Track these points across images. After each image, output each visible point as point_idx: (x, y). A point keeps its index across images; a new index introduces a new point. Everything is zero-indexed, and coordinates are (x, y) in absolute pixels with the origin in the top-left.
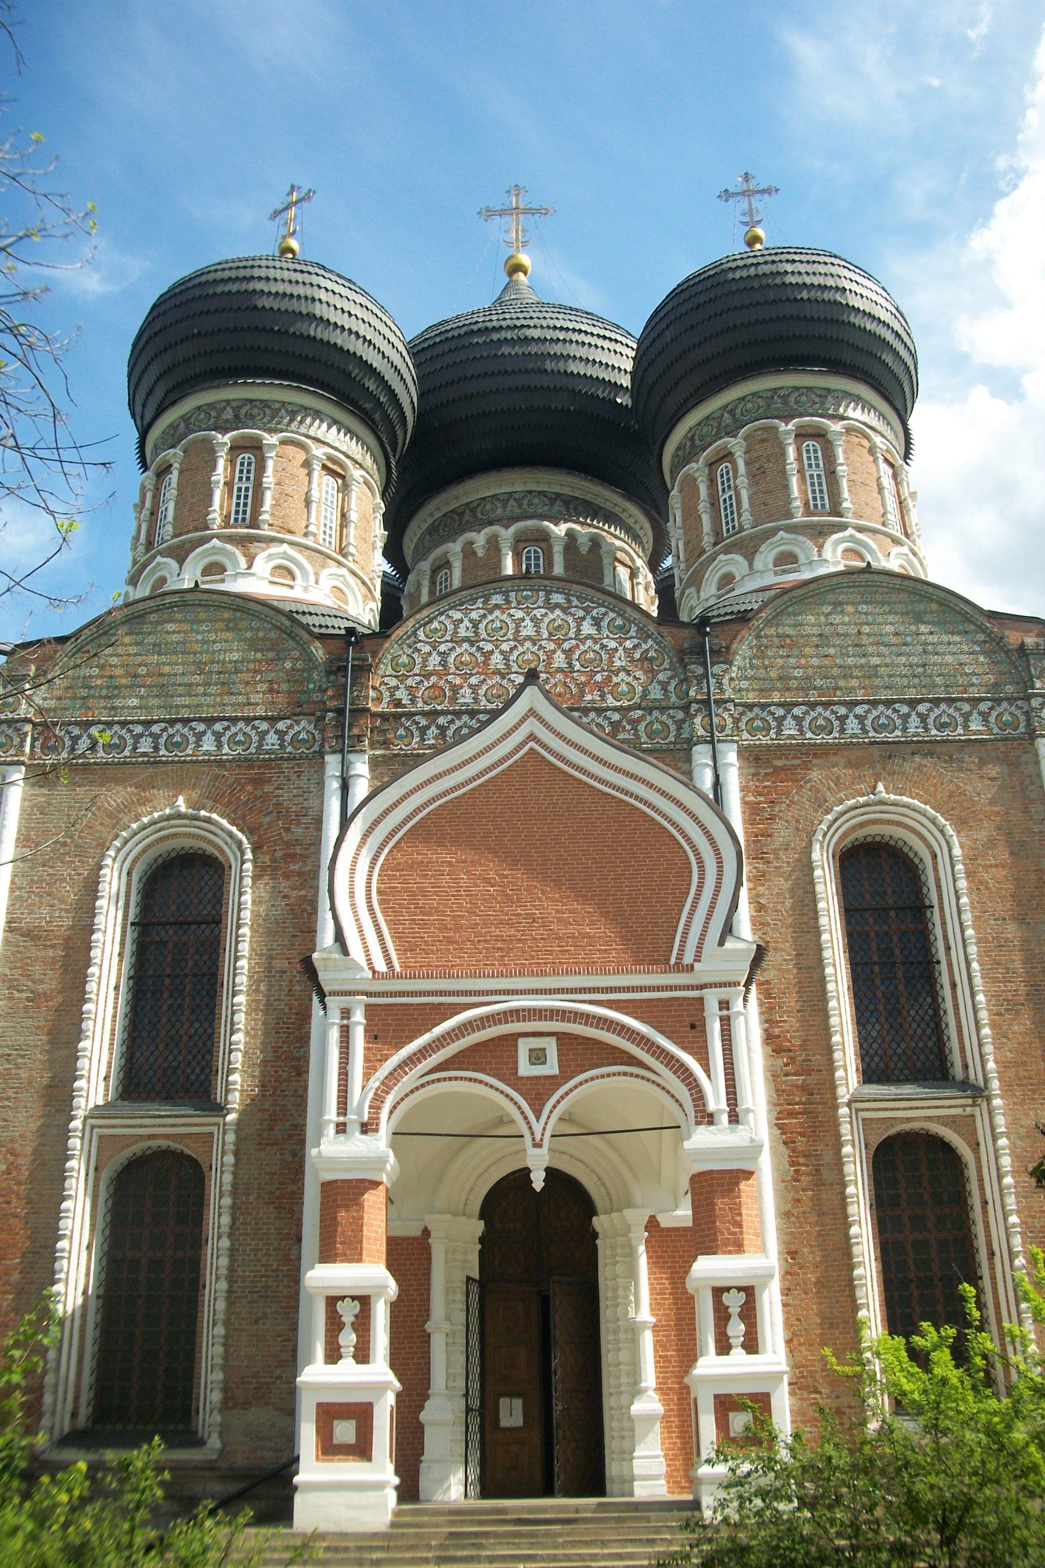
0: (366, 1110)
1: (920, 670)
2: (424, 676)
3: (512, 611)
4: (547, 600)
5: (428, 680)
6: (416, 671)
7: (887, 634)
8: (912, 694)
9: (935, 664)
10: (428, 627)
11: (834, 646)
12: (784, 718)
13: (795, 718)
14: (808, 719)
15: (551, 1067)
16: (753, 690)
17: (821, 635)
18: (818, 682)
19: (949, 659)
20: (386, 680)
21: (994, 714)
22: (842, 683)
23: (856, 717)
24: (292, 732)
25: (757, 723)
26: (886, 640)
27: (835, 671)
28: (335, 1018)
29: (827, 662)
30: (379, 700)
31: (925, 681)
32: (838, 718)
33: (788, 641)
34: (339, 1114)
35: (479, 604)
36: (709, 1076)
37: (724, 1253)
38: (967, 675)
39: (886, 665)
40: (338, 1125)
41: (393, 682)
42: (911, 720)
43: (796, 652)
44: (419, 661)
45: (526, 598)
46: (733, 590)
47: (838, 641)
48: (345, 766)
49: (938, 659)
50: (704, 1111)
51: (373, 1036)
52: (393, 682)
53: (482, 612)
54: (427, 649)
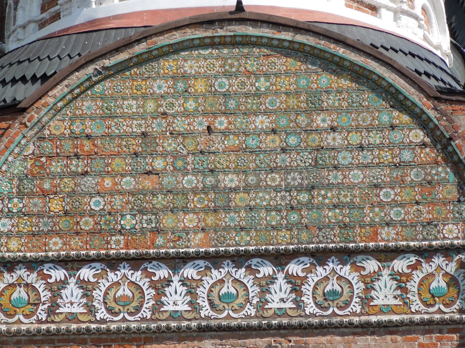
1: (304, 197)
7: (258, 133)
8: (283, 241)
9: (329, 186)
11: (164, 155)
12: (63, 283)
13: (83, 284)
14: (104, 284)
16: (19, 235)
17: (144, 134)
18: (128, 222)
19: (356, 176)
21: (418, 276)
22: (168, 221)
23: (183, 282)
25: (20, 293)
26: (252, 142)
27: (160, 201)
29: (148, 183)
31: (309, 216)
32: (153, 285)
33: (87, 146)
38: (381, 205)
42: (274, 287)
43: (98, 165)
46: (56, 17)
47: (170, 145)
49: (334, 177)
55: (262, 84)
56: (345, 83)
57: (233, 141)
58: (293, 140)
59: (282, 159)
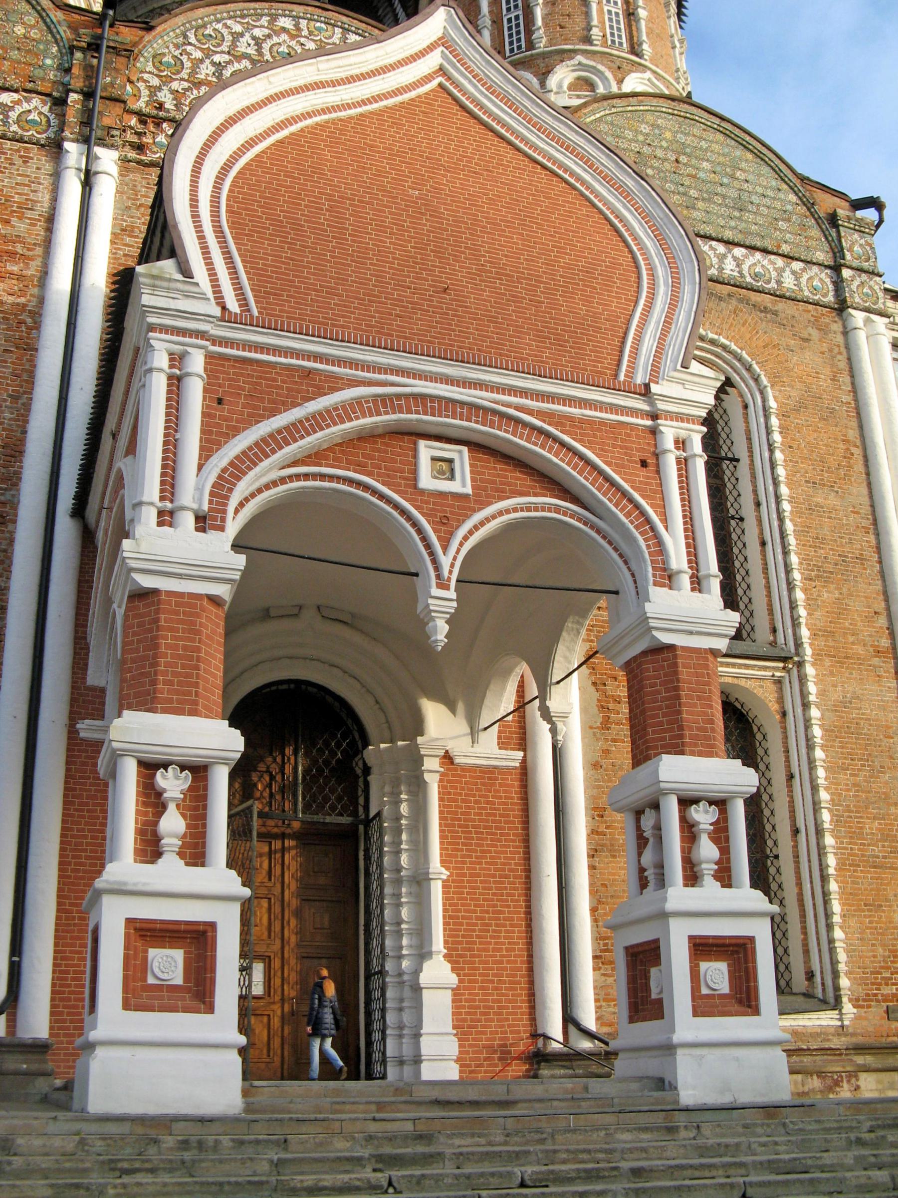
0: (206, 497)
2: (194, 84)
3: (302, 40)
4: (344, 39)
5: (198, 89)
6: (184, 74)
8: (728, 234)
10: (200, 31)
15: (463, 484)
20: (146, 76)
24: (19, 109)
28: (160, 360)
30: (137, 96)
34: (162, 499)
35: (264, 21)
36: (666, 528)
37: (692, 754)
39: (703, 199)
40: (161, 513)
41: (155, 82)
44: (187, 64)
45: (319, 30)
48: (90, 157)
50: (665, 570)
51: (215, 399)
52: (155, 82)
53: (267, 31)
54: (198, 54)
55: (704, 144)
56: (750, 156)
57: (690, 170)
58: (725, 180)
59: (719, 190)
